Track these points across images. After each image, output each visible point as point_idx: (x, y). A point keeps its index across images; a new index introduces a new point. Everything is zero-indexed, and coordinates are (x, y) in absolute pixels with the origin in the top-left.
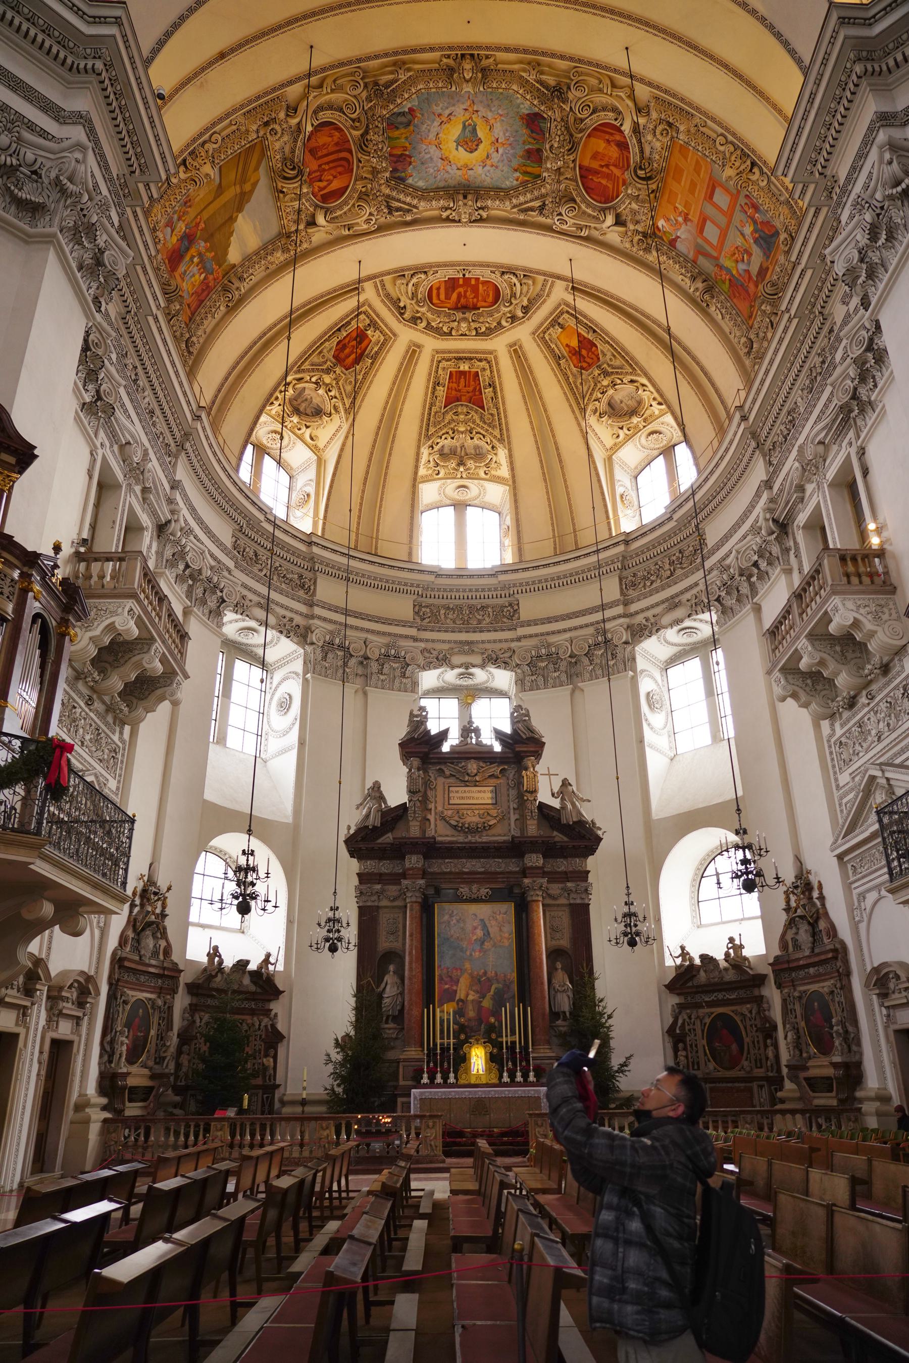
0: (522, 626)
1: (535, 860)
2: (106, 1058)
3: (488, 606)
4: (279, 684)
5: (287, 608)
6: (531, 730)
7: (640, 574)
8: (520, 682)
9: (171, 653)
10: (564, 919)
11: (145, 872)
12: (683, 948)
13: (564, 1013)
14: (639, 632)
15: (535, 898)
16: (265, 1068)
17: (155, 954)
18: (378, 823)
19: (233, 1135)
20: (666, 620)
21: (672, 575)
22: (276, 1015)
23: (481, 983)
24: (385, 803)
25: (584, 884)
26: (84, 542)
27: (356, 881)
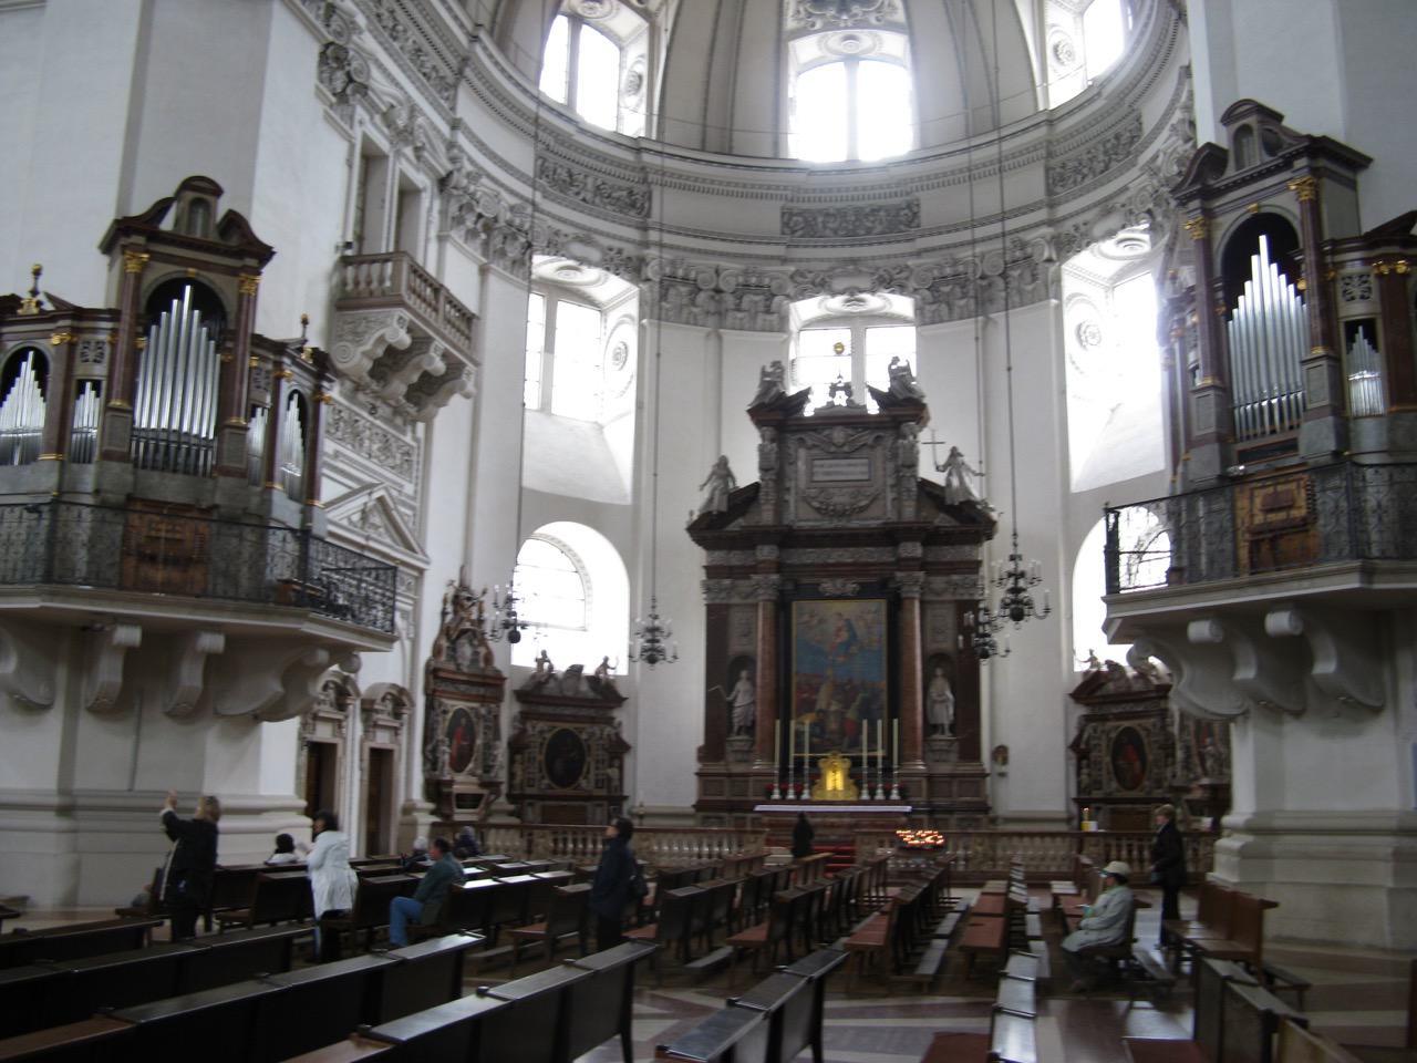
0: (922, 236)
1: (914, 550)
2: (429, 766)
3: (879, 209)
4: (614, 330)
5: (614, 237)
6: (911, 390)
7: (1070, 165)
8: (919, 310)
9: (454, 346)
10: (946, 617)
11: (455, 576)
12: (1091, 652)
13: (942, 725)
14: (1068, 244)
15: (910, 595)
16: (609, 779)
17: (474, 661)
18: (724, 508)
19: (555, 841)
20: (1098, 230)
21: (1107, 168)
22: (620, 724)
23: (845, 692)
24: (734, 481)
25: (973, 577)
26: (348, 245)
27: (702, 575)
